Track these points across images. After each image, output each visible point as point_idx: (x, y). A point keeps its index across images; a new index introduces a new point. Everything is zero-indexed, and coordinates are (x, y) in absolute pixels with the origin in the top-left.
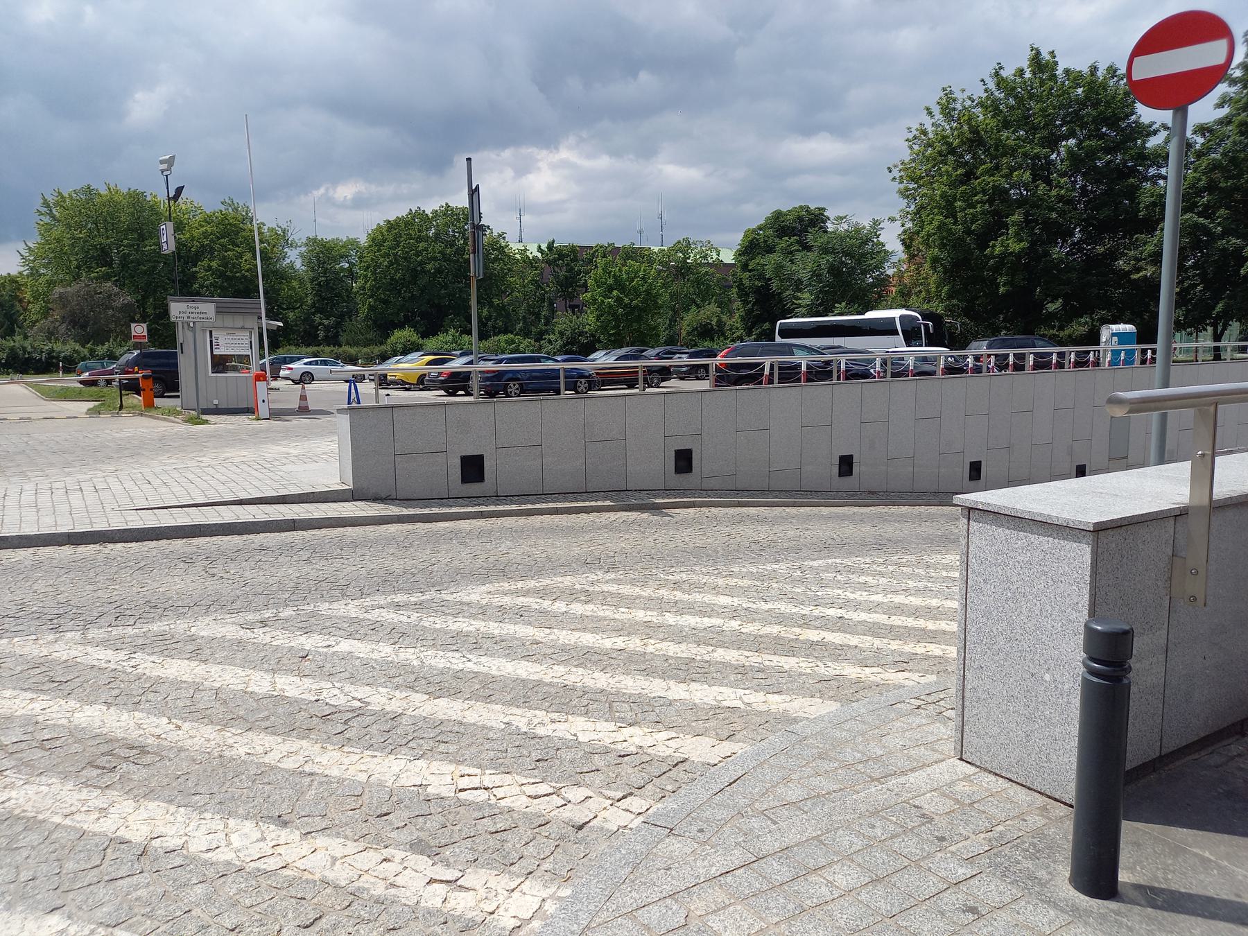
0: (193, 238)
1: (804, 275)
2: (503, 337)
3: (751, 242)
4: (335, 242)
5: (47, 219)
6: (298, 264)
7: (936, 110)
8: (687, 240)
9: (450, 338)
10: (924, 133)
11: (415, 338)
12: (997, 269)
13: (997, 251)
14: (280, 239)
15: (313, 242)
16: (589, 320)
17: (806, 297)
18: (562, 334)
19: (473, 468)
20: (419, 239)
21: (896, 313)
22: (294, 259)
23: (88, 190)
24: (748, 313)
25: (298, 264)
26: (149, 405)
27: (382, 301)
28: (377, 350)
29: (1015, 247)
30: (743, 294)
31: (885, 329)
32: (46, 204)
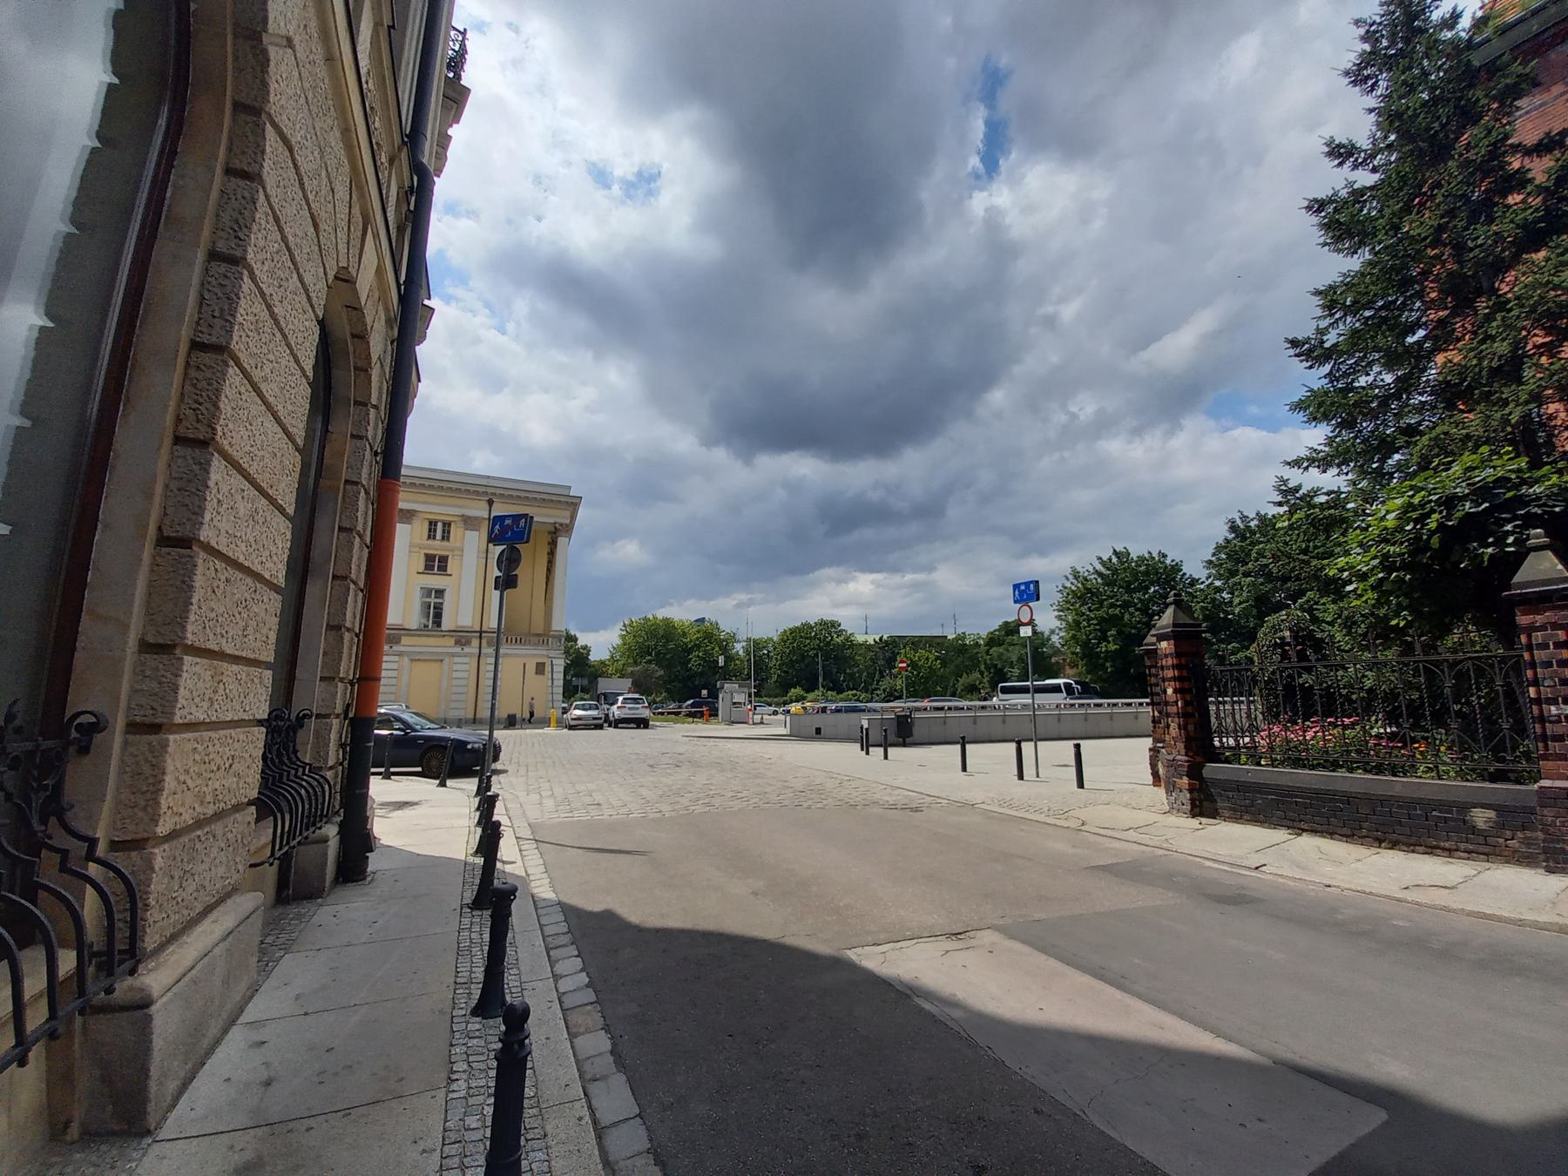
0: (691, 641)
1: (1014, 659)
2: (850, 692)
3: (990, 639)
4: (761, 639)
5: (624, 633)
6: (741, 652)
7: (1071, 577)
8: (964, 633)
9: (820, 694)
10: (1065, 588)
11: (802, 693)
12: (1106, 659)
13: (1103, 650)
14: (733, 638)
15: (749, 640)
16: (900, 683)
17: (1016, 671)
18: (884, 690)
19: (818, 731)
20: (807, 638)
21: (1061, 681)
22: (739, 648)
23: (645, 619)
24: (992, 678)
25: (741, 652)
26: (707, 720)
27: (786, 672)
28: (782, 700)
29: (1112, 647)
30: (988, 668)
31: (1056, 689)
32: (624, 626)
